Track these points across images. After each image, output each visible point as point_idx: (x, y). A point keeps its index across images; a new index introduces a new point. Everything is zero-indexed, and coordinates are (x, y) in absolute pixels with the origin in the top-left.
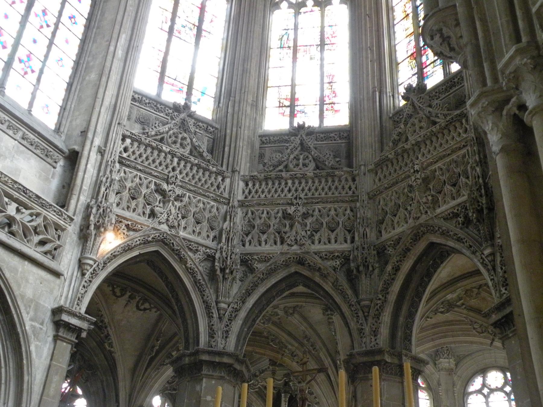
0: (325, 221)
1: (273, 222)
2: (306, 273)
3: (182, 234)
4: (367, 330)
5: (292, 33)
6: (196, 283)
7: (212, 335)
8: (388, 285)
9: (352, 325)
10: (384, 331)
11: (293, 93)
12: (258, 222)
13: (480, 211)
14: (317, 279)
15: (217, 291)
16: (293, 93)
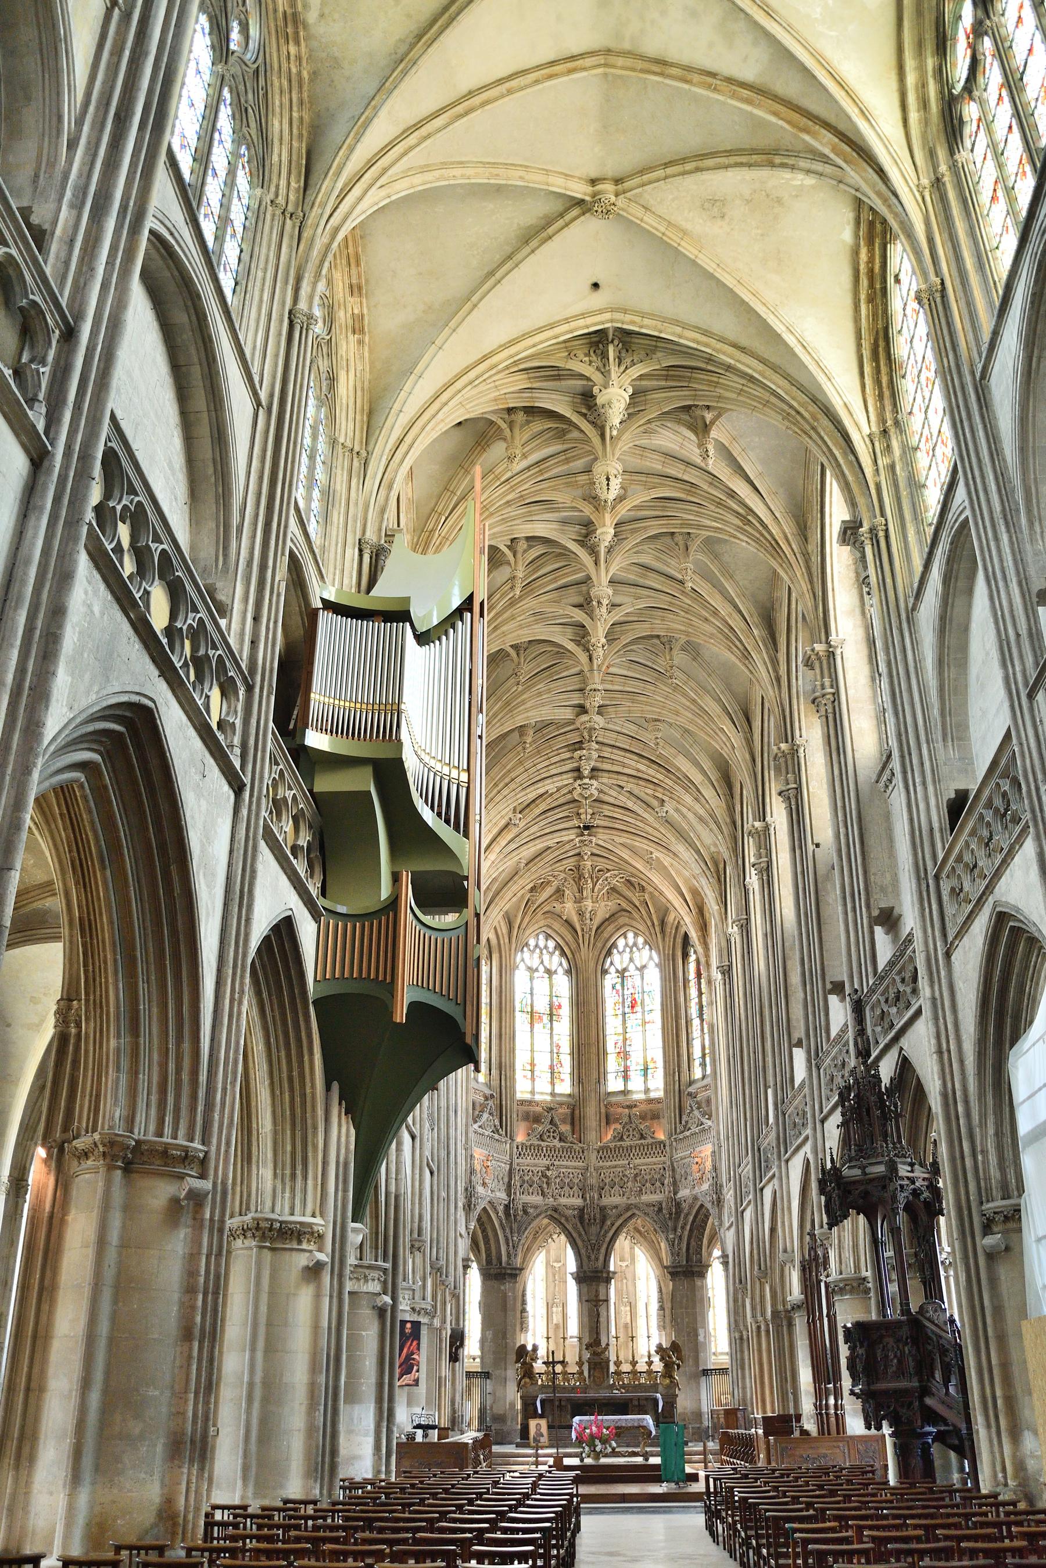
0: (567, 1181)
1: (536, 1179)
2: (556, 1216)
3: (498, 1194)
4: (593, 1257)
5: (529, 996)
6: (501, 1224)
7: (509, 1255)
8: (607, 1232)
9: (583, 1251)
10: (601, 1258)
11: (533, 1059)
12: (526, 1178)
13: (671, 1214)
14: (563, 1220)
15: (511, 1229)
16: (533, 1059)
